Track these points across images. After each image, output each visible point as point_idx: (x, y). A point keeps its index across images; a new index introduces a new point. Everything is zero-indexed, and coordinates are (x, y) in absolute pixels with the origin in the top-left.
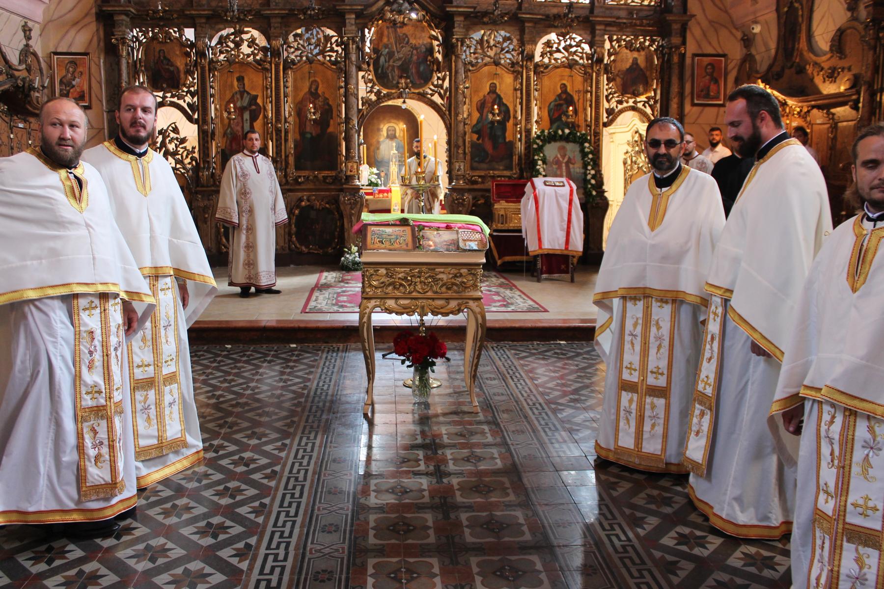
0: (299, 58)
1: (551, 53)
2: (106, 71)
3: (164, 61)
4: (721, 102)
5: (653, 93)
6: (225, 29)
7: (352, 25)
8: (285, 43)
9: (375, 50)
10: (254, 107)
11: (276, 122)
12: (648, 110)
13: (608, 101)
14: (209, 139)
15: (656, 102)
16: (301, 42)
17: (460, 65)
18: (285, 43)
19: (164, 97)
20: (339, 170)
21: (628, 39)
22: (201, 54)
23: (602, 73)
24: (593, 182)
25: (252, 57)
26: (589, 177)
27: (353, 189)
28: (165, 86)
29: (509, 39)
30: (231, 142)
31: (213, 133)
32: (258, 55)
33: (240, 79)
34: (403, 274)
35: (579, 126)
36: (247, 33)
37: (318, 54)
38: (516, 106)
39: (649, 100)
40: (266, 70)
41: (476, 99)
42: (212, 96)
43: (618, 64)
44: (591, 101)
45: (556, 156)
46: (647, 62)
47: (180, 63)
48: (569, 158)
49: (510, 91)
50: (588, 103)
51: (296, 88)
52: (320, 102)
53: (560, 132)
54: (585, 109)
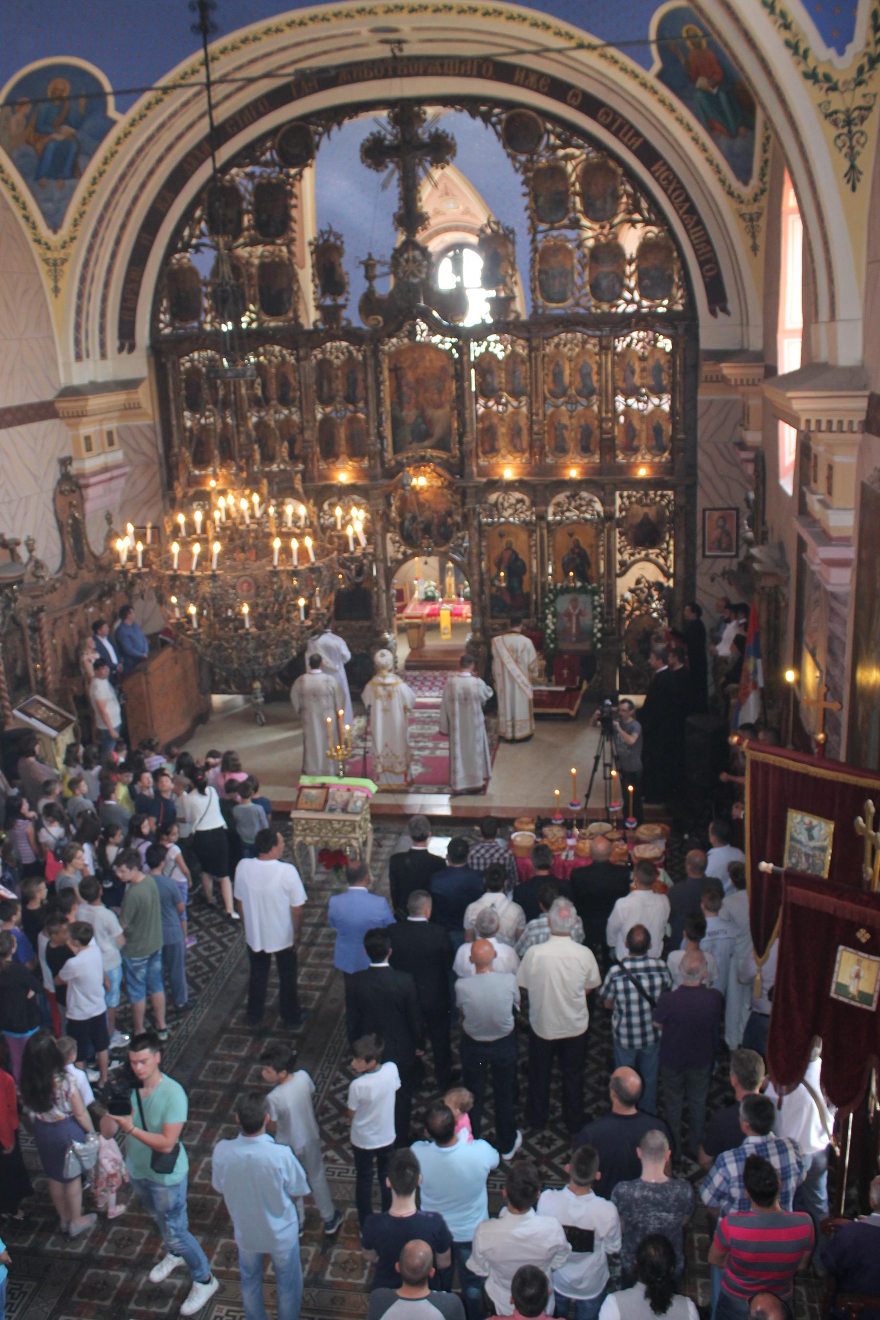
1: (563, 513)
4: (733, 553)
9: (401, 514)
12: (661, 561)
13: (621, 553)
26: (595, 630)
38: (530, 562)
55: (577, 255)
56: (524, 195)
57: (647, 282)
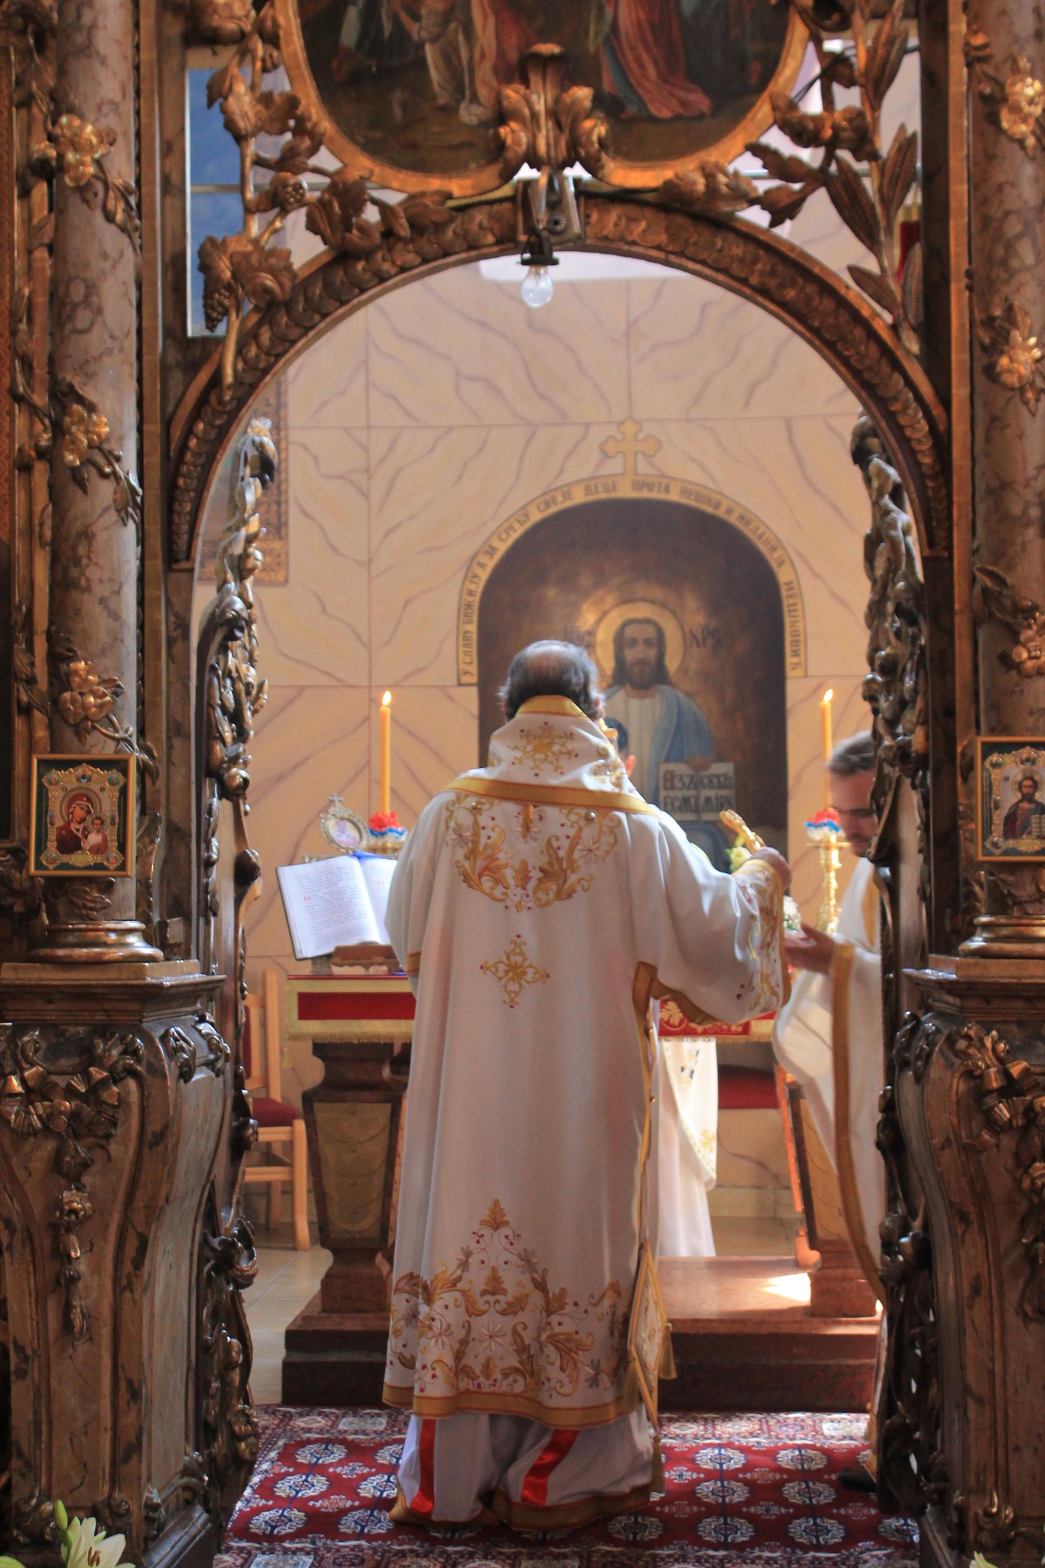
27: (83, 994)
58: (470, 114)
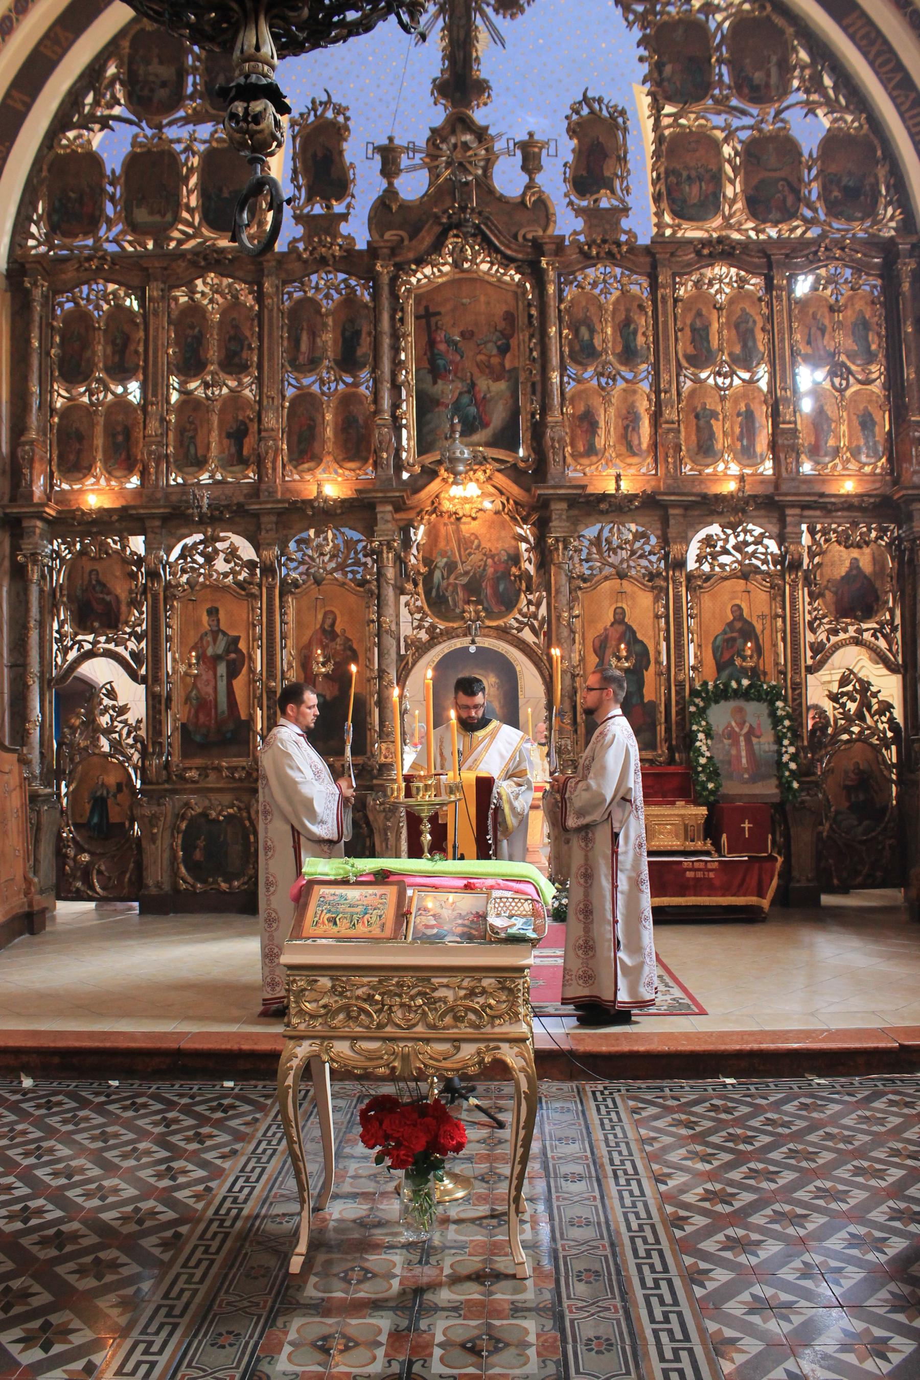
0: (304, 577)
2: (10, 604)
3: (98, 588)
5: (887, 614)
6: (191, 535)
7: (387, 521)
8: (282, 555)
9: (428, 561)
10: (233, 656)
11: (267, 678)
13: (813, 631)
14: (163, 707)
15: (894, 629)
16: (310, 552)
17: (563, 579)
18: (282, 555)
19: (95, 643)
20: (369, 754)
21: (840, 529)
22: (153, 575)
23: (800, 586)
24: (793, 766)
25: (231, 577)
26: (785, 758)
28: (96, 624)
29: (643, 535)
30: (197, 713)
31: (169, 699)
32: (240, 574)
33: (213, 612)
34: (364, 989)
35: (765, 674)
36: (223, 540)
37: (335, 570)
38: (658, 644)
39: (882, 627)
40: (253, 596)
41: (591, 635)
42: (169, 639)
43: (827, 570)
44: (784, 632)
45: (729, 725)
46: (874, 565)
47: (121, 589)
48: (751, 726)
49: (649, 619)
50: (779, 635)
51: (300, 624)
52: (338, 645)
53: (734, 684)
54: (775, 645)
55: (727, 150)
56: (641, 59)
57: (836, 193)
58: (458, 611)
